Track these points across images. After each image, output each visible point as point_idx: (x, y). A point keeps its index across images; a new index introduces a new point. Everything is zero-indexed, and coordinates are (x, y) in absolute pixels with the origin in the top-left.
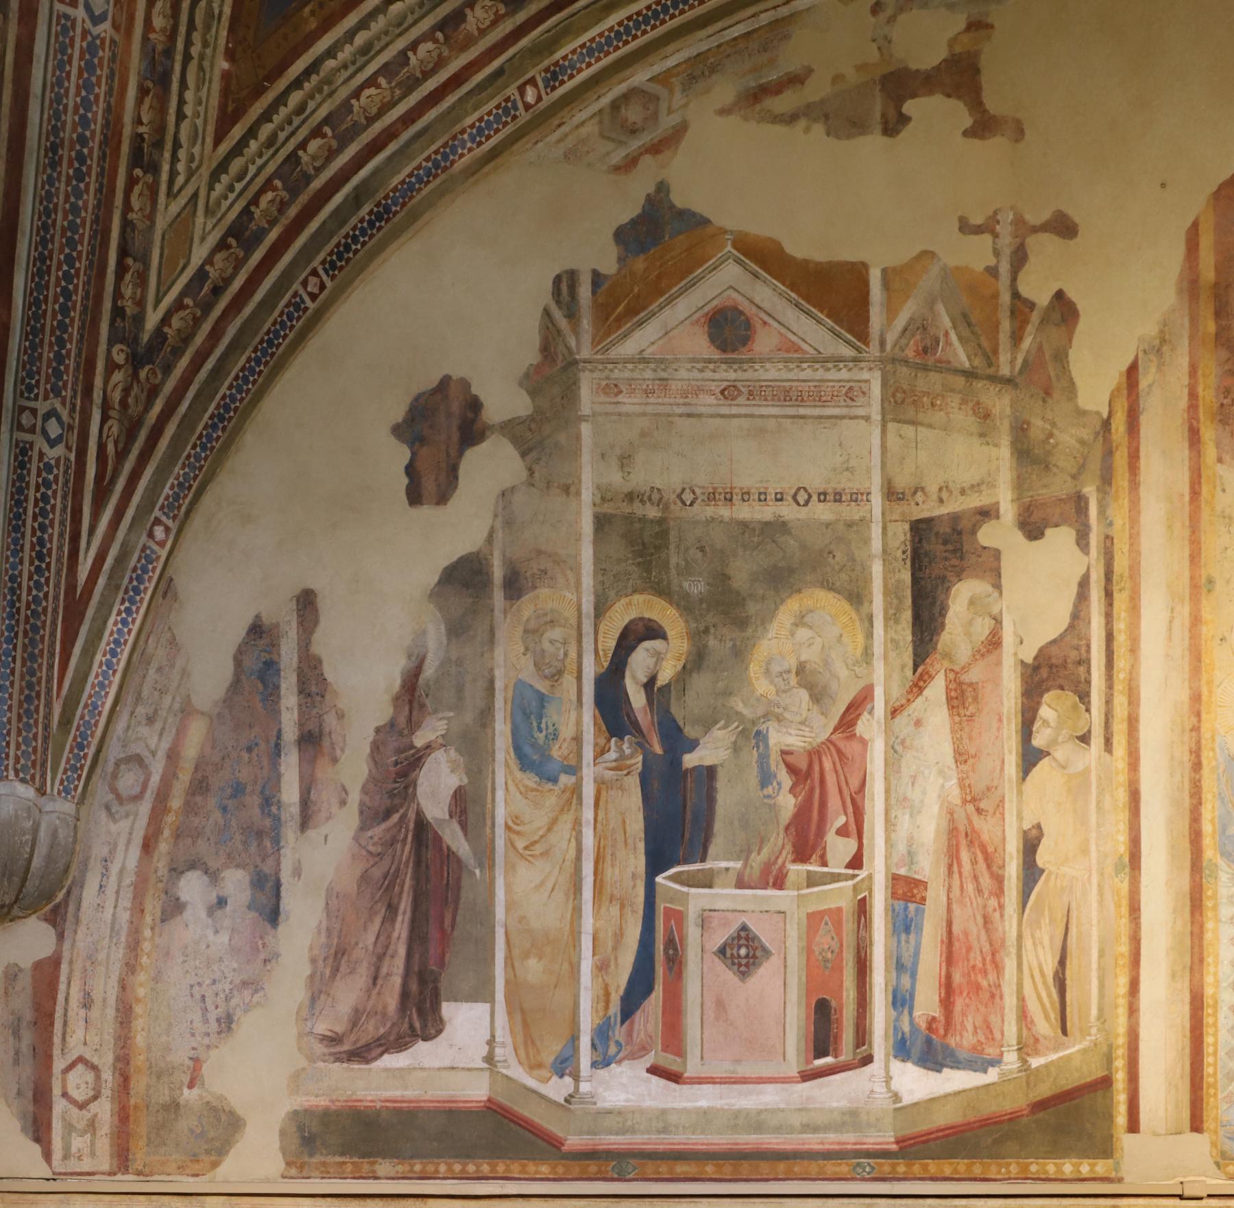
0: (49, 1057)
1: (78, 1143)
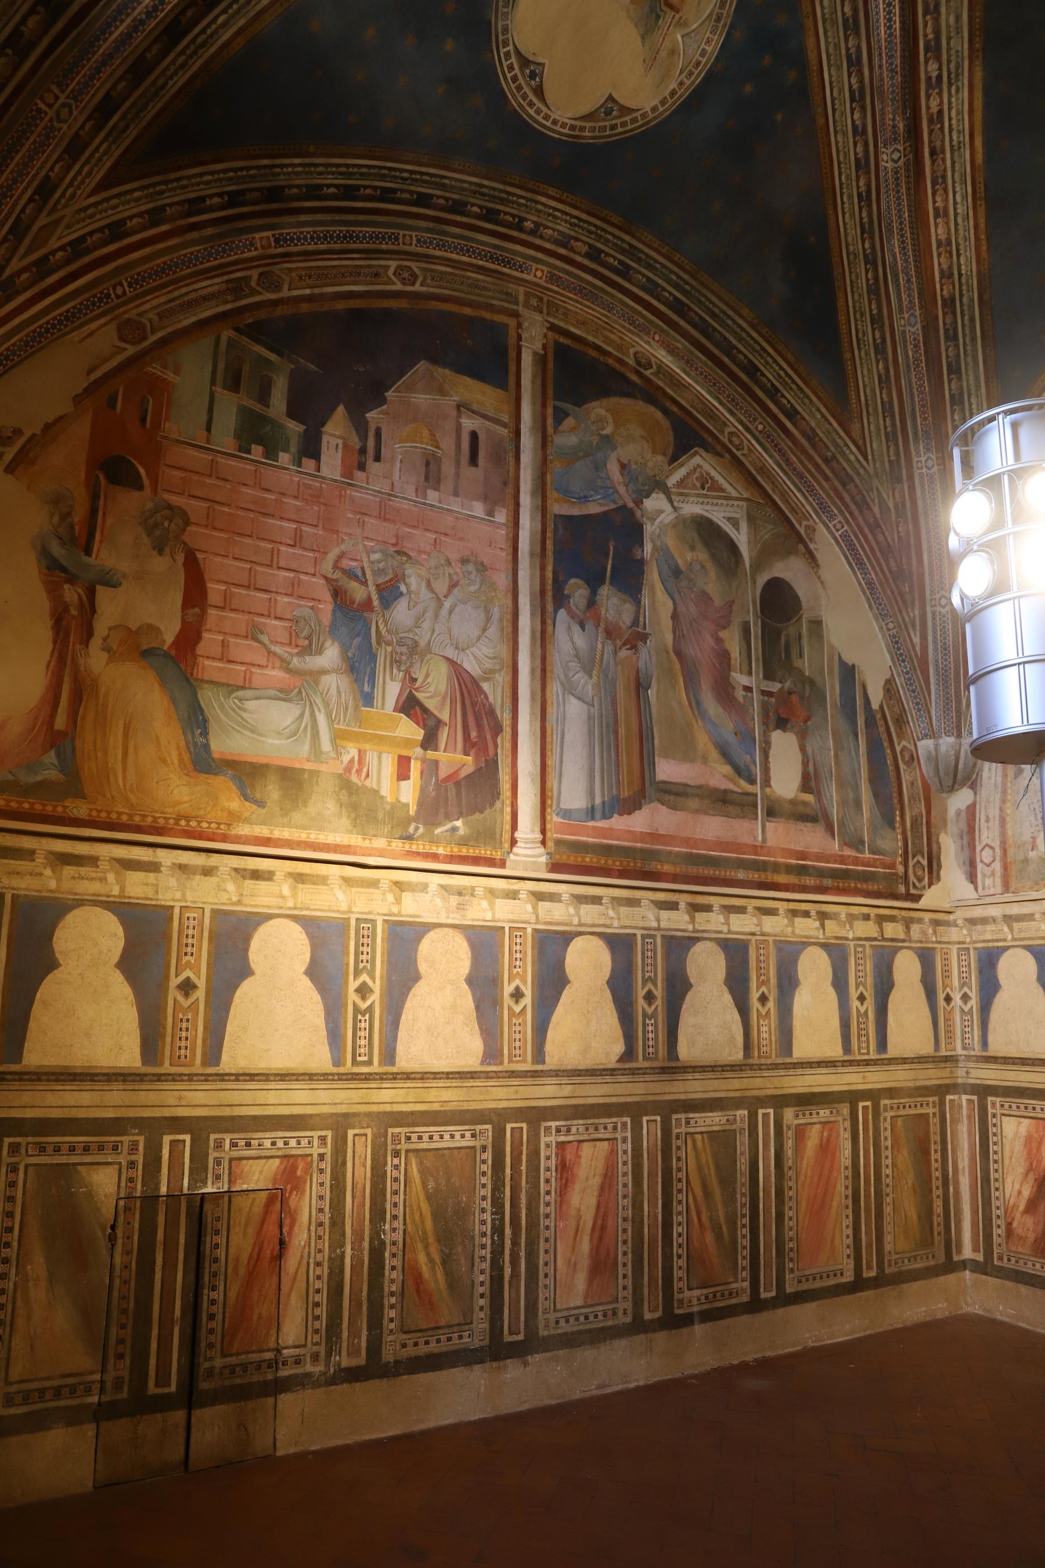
0: (974, 846)
1: (988, 882)
